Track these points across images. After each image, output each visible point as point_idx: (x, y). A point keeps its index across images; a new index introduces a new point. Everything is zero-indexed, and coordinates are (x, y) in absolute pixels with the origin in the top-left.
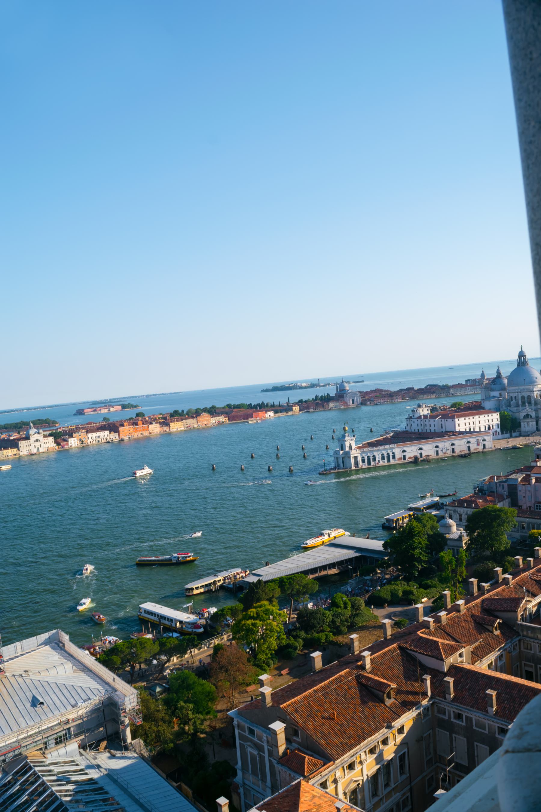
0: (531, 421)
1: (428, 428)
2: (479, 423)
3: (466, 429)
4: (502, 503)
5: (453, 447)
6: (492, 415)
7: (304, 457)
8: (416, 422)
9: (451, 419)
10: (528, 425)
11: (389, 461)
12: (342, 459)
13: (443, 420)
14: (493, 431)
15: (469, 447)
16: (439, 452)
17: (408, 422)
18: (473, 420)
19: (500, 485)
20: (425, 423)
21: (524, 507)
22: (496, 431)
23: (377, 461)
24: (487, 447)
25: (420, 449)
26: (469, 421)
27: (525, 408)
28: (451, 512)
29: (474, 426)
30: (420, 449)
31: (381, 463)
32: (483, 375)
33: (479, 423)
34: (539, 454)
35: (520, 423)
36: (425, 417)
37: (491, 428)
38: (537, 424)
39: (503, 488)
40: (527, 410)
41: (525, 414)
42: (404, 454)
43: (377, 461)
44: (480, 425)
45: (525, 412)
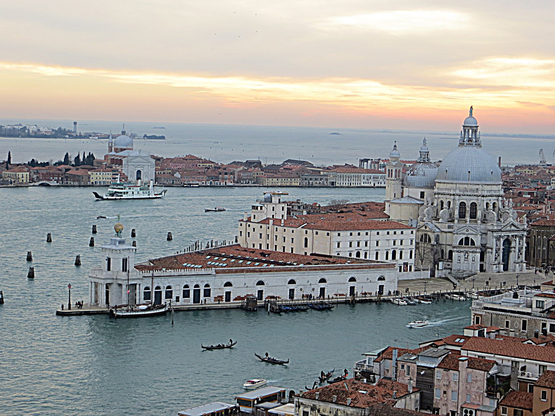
0: (472, 252)
1: (279, 243)
3: (350, 255)
4: (403, 400)
5: (322, 285)
6: (402, 233)
7: (31, 276)
10: (466, 259)
11: (197, 299)
12: (107, 287)
14: (401, 262)
15: (352, 288)
16: (295, 291)
17: (243, 229)
19: (403, 366)
22: (406, 264)
23: (174, 299)
24: (385, 292)
25: (261, 283)
26: (358, 238)
28: (306, 410)
29: (367, 248)
30: (261, 283)
31: (183, 302)
34: (481, 315)
35: (451, 252)
36: (277, 222)
37: (398, 256)
38: (482, 259)
41: (464, 237)
42: (228, 289)
43: (174, 299)
44: (377, 248)
45: (464, 234)
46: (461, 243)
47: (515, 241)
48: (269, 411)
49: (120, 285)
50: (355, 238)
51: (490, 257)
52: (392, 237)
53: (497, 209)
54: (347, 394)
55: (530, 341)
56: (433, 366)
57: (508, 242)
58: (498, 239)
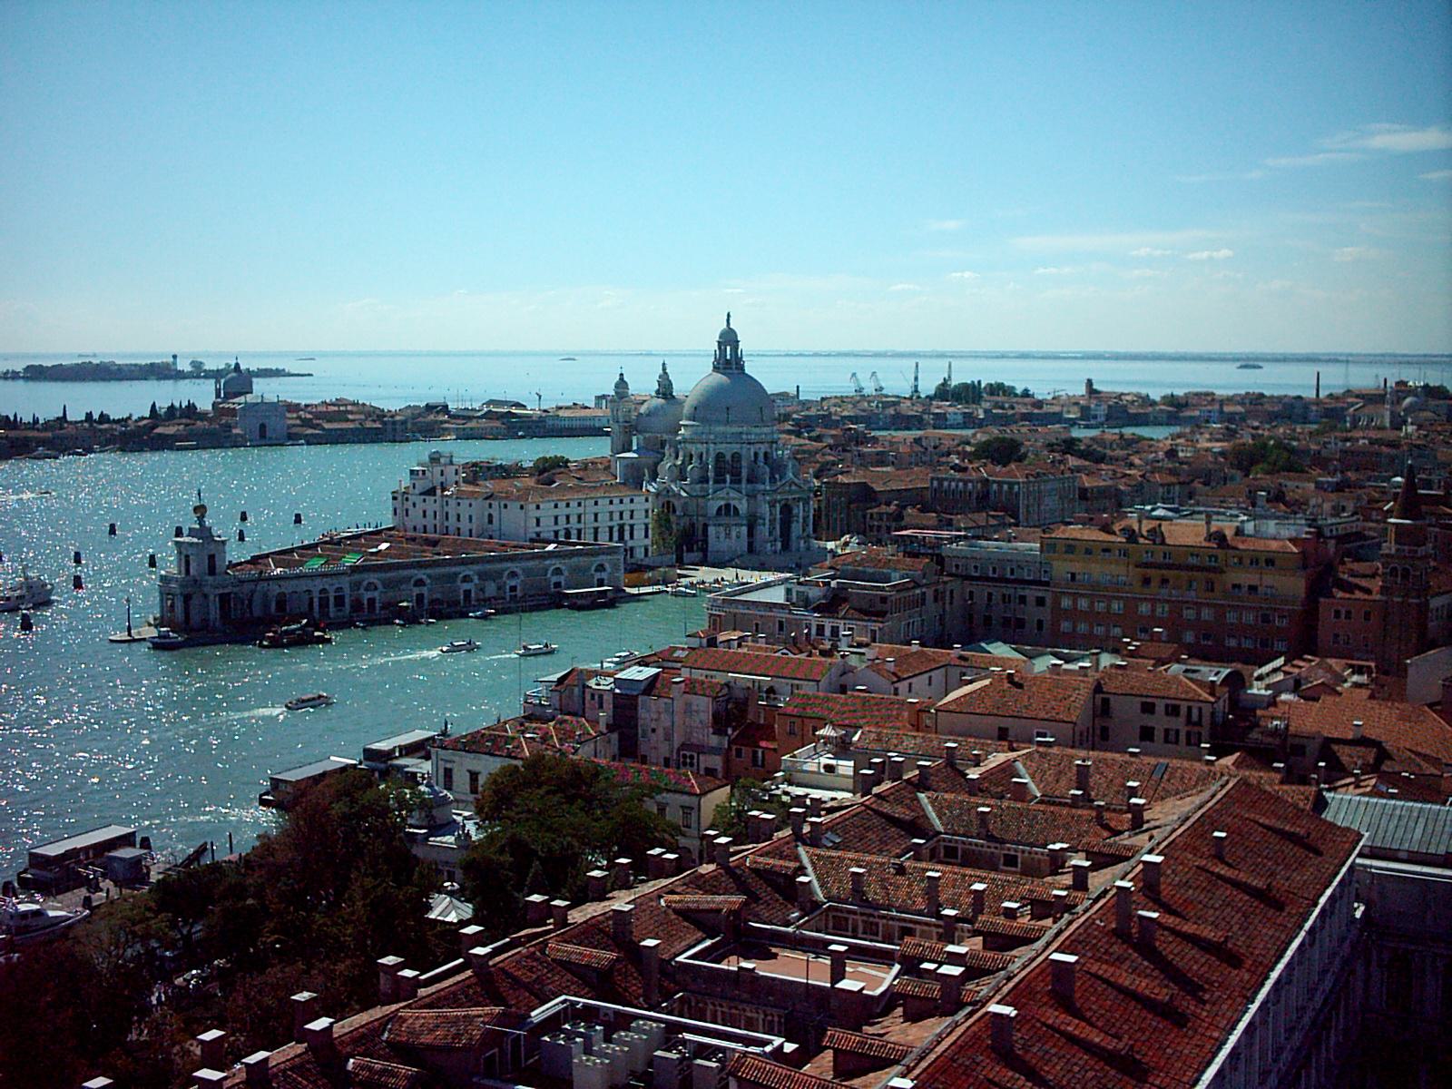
2: (596, 520)
6: (632, 501)
8: (421, 506)
9: (518, 504)
10: (728, 535)
13: (495, 504)
17: (398, 503)
18: (581, 510)
19: (593, 695)
20: (446, 509)
21: (652, 756)
27: (723, 485)
28: (448, 766)
32: (622, 384)
33: (596, 520)
34: (719, 616)
35: (706, 526)
38: (751, 534)
39: (601, 706)
40: (728, 494)
41: (723, 503)
44: (596, 525)
45: (723, 498)
46: (720, 509)
47: (798, 506)
48: (406, 769)
49: (206, 596)
50: (562, 510)
51: (763, 531)
52: (616, 507)
53: (771, 461)
54: (508, 740)
55: (785, 651)
56: (635, 693)
57: (787, 510)
58: (772, 504)
